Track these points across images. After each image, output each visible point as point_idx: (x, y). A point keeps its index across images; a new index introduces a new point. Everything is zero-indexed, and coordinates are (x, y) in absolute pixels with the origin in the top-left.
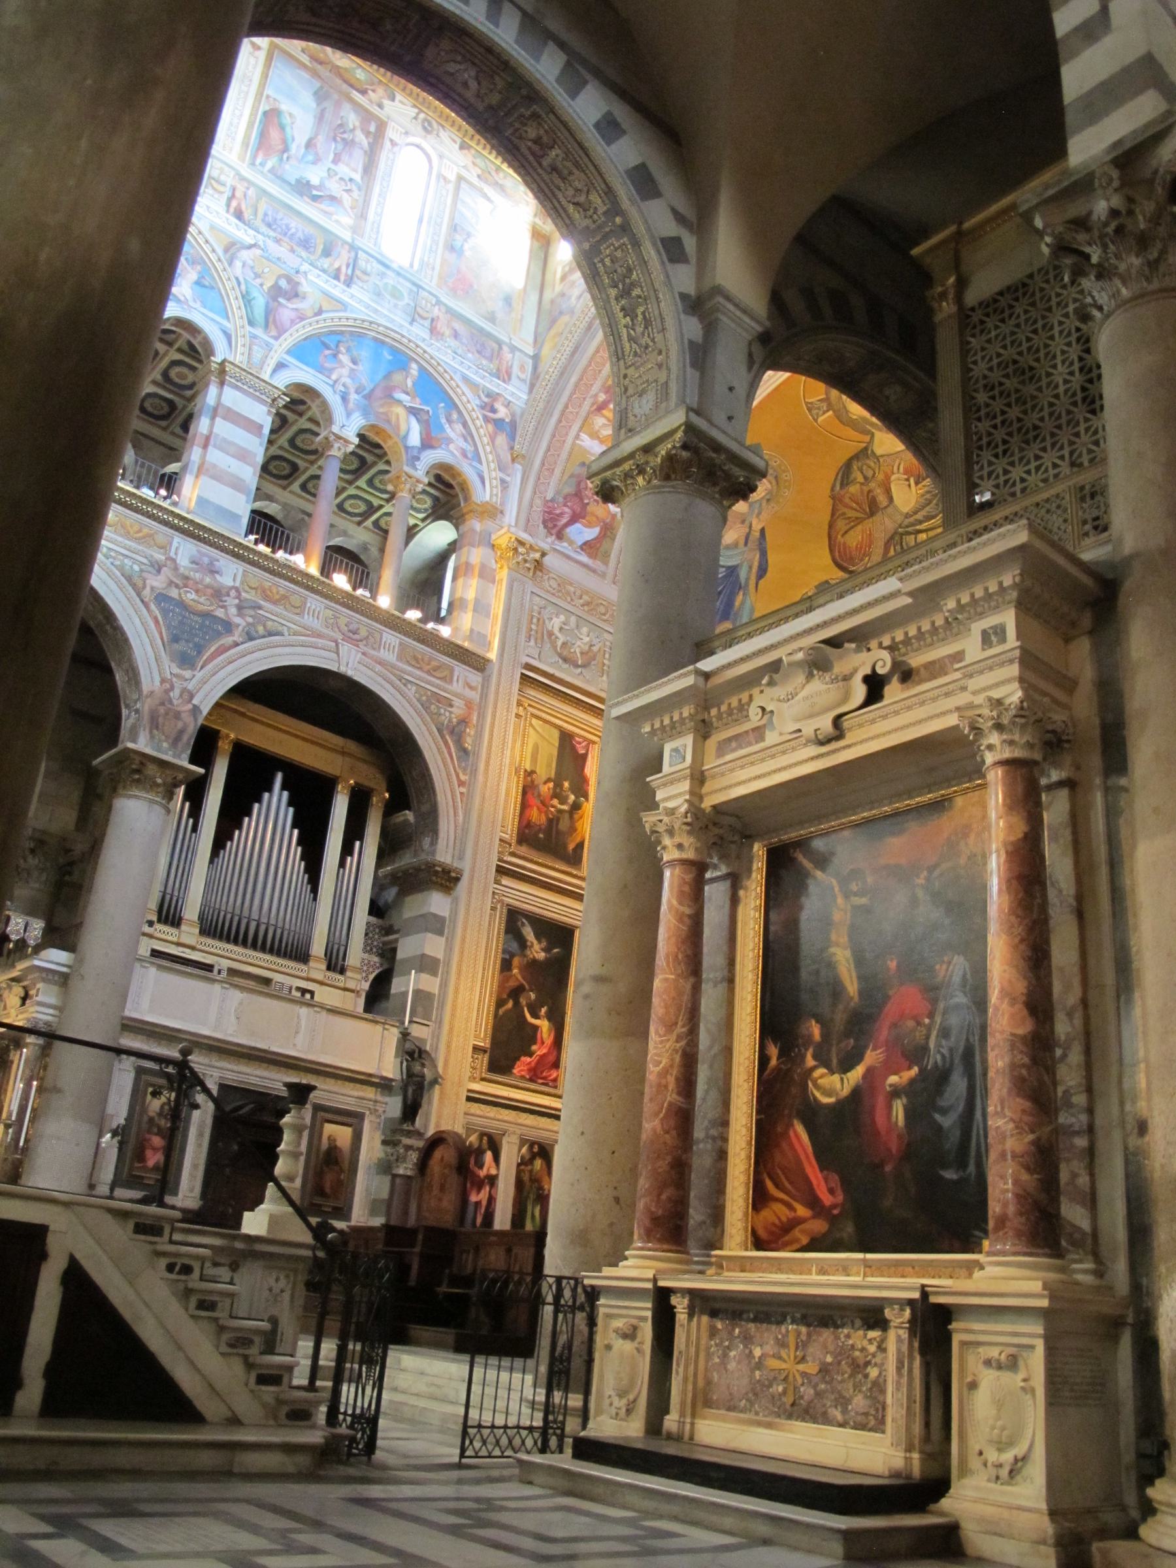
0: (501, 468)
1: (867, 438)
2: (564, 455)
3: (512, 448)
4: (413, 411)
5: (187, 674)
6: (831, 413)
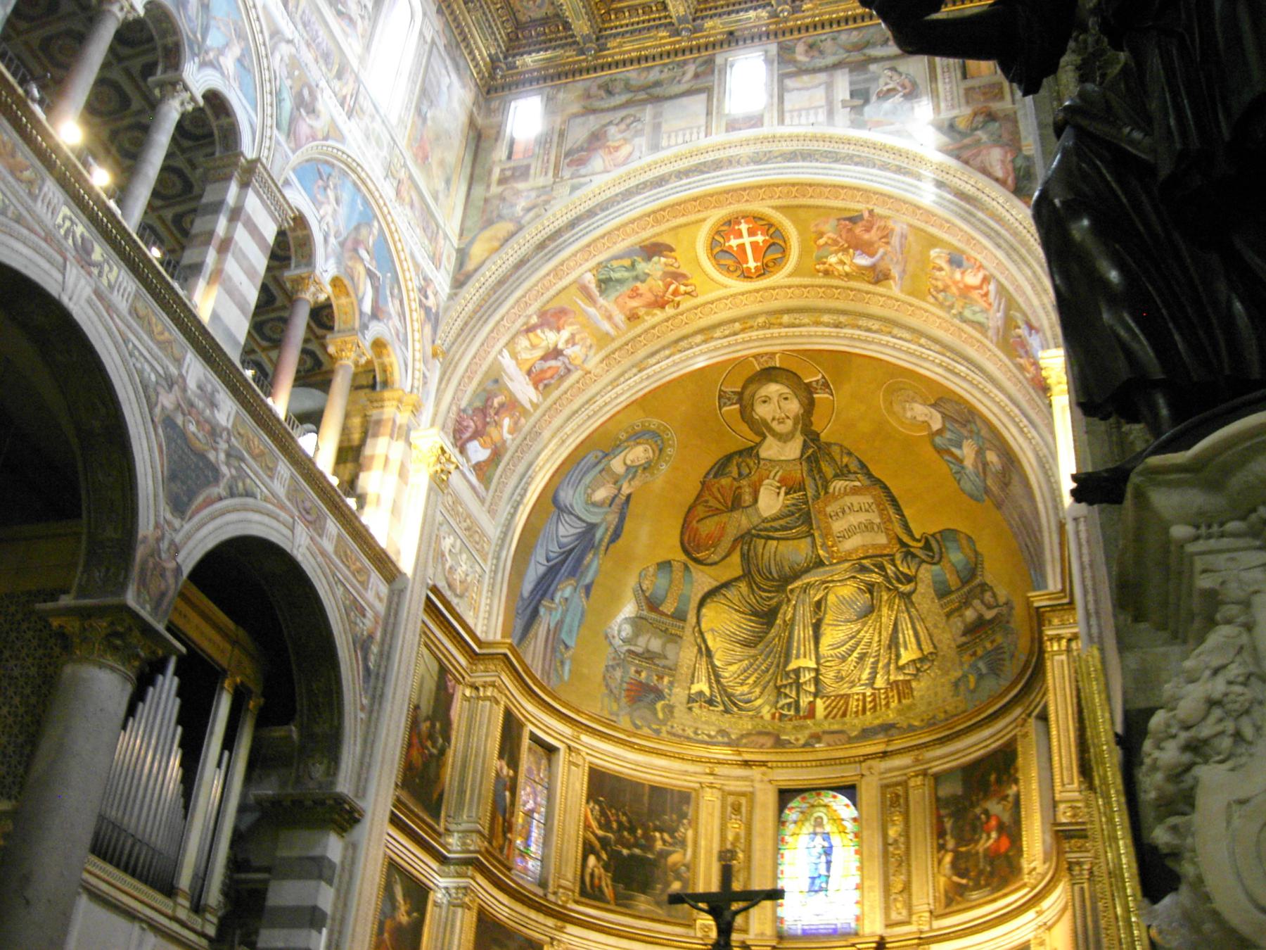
0: (425, 362)
1: (758, 439)
2: (484, 367)
3: (433, 342)
4: (370, 274)
5: (177, 523)
6: (737, 406)
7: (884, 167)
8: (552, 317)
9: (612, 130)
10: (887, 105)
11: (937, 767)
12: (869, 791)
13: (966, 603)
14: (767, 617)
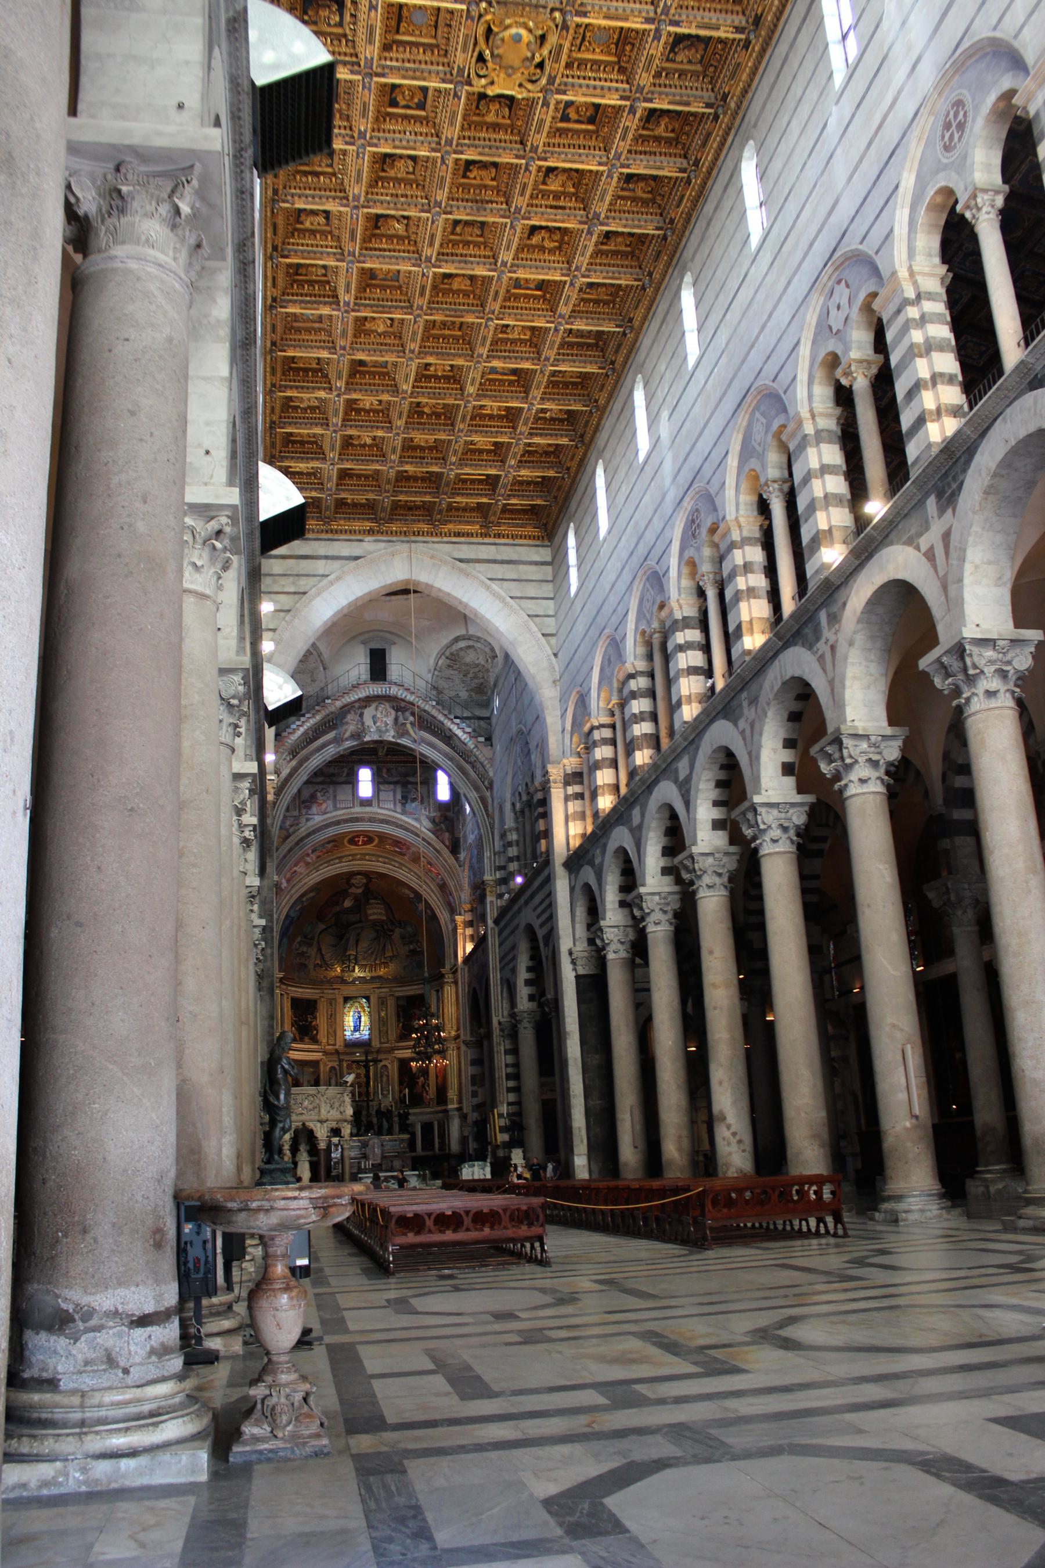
7: (412, 832)
8: (296, 865)
9: (319, 794)
10: (414, 805)
11: (397, 994)
12: (373, 999)
13: (411, 943)
14: (340, 937)
